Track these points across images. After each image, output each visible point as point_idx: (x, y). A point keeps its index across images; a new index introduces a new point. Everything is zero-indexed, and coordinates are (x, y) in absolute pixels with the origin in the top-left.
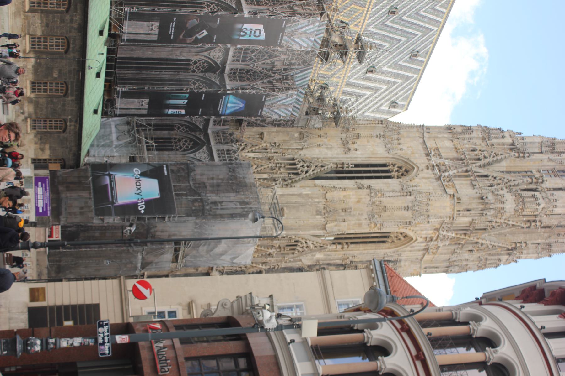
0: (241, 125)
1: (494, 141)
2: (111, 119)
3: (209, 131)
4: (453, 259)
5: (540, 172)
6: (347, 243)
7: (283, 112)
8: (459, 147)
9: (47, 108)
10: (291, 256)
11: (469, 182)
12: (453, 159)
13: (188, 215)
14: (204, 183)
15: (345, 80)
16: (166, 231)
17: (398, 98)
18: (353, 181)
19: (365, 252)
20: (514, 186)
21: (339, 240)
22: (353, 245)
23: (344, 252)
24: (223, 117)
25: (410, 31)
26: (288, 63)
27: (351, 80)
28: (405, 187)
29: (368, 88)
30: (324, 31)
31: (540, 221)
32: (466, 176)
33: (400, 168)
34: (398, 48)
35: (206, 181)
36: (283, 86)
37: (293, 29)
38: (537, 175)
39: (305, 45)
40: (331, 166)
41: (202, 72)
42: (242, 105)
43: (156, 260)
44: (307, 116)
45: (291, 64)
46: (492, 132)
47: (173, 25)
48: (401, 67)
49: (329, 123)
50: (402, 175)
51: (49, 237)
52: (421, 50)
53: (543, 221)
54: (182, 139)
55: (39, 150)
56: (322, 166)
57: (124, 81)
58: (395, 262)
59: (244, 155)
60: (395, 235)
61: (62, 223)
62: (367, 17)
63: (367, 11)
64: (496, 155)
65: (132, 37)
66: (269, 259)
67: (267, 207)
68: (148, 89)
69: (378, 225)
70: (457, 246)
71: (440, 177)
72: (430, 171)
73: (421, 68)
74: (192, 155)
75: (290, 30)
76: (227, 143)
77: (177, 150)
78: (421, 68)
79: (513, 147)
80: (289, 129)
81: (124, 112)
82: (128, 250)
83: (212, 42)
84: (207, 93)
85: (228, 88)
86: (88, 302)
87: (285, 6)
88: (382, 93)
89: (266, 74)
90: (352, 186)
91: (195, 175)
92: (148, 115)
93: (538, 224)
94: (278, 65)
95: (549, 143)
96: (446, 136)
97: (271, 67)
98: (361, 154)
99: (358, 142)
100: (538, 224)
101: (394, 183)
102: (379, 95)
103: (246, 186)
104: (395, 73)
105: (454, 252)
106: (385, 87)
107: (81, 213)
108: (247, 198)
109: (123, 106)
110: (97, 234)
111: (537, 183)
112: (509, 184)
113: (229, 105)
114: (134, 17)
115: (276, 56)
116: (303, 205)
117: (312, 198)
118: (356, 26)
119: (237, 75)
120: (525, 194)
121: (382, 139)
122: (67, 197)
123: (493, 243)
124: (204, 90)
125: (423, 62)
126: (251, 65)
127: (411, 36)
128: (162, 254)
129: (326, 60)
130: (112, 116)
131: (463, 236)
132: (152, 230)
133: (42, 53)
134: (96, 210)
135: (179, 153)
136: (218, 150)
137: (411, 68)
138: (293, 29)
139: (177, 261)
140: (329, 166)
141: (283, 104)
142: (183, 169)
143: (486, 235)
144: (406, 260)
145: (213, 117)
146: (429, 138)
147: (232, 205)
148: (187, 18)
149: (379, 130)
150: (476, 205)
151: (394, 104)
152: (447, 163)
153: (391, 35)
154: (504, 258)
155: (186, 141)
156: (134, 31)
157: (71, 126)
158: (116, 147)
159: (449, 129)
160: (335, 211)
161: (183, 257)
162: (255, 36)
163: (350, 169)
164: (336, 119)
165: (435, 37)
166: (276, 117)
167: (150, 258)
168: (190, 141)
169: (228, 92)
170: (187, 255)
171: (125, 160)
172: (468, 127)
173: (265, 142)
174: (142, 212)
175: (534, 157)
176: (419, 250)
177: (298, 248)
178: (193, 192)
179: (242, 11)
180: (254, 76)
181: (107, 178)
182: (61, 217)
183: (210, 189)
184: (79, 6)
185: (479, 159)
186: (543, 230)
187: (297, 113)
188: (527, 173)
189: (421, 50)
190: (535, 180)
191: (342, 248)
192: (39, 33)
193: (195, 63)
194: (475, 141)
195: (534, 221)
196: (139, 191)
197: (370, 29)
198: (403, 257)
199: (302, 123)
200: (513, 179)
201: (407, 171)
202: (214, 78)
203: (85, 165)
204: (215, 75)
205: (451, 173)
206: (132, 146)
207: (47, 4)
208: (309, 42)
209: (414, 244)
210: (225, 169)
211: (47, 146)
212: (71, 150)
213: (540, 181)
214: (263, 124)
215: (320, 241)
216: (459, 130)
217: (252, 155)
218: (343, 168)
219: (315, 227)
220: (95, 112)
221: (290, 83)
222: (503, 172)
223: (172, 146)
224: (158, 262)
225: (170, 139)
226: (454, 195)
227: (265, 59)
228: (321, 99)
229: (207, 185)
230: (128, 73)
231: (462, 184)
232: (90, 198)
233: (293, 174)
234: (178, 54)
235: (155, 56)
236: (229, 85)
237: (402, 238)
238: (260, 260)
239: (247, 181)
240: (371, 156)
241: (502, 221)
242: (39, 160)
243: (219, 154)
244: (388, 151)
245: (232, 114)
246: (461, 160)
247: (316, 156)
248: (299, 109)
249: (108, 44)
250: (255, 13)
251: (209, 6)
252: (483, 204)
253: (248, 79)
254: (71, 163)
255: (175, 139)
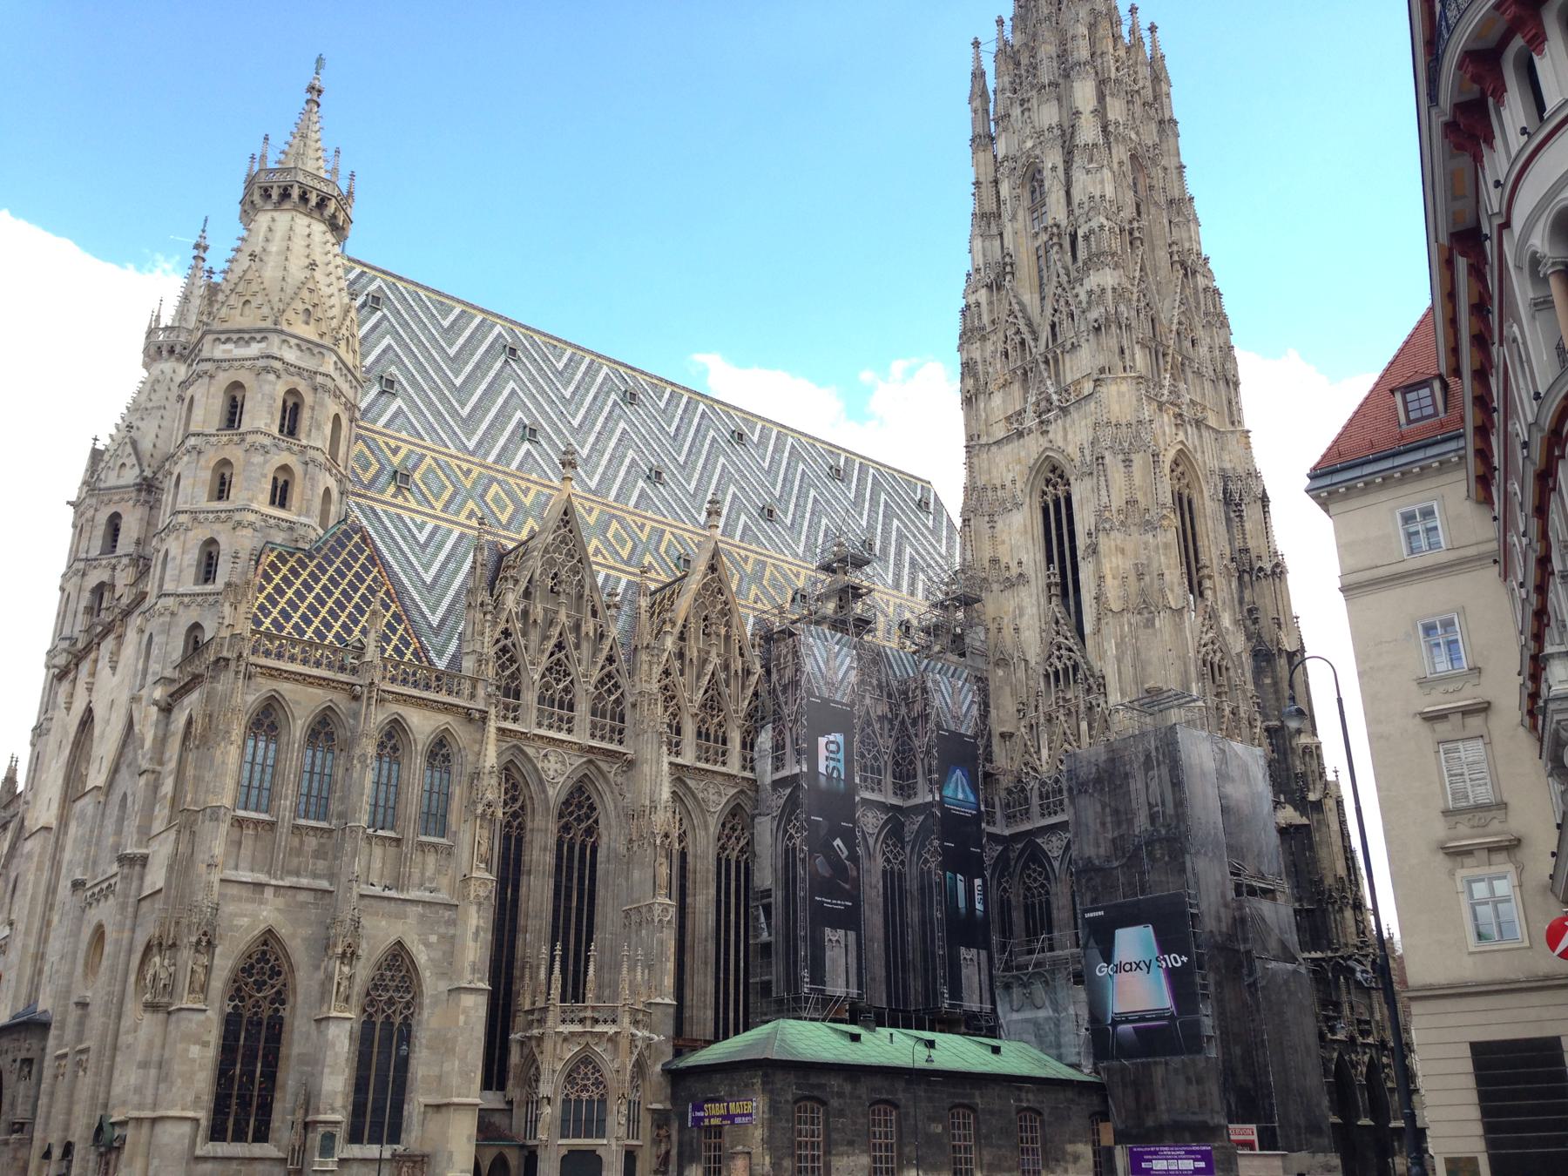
0: (992, 775)
1: (986, 319)
2: (1002, 1021)
3: (1007, 832)
4: (1212, 373)
5: (1037, 234)
6: (1198, 570)
7: (965, 698)
8: (1001, 381)
9: (999, 1147)
10: (1232, 673)
11: (1067, 356)
12: (1026, 390)
13: (1183, 870)
14: (1114, 840)
15: (890, 591)
16: (1218, 912)
17: (912, 499)
18: (1082, 565)
19: (1211, 535)
20: (1068, 276)
21: (1196, 586)
22: (1201, 557)
23: (1216, 575)
24: (983, 808)
25: (797, 483)
26: (878, 692)
27: (890, 582)
28: (1085, 469)
29: (899, 553)
30: (819, 628)
31: (1131, 222)
32: (1056, 361)
33: (1048, 482)
34: (827, 501)
35: (1110, 836)
36: (919, 698)
37: (822, 683)
38: (1045, 237)
39: (848, 659)
40: (1056, 606)
41: (903, 848)
42: (958, 772)
43: (1277, 931)
44: (968, 654)
45: (880, 686)
46: (969, 325)
47: (828, 903)
48: (860, 494)
49: (975, 615)
50: (1061, 476)
51: (1252, 1148)
52: (827, 463)
53: (1130, 217)
54: (1025, 883)
55: (1078, 1165)
56: (1057, 622)
57: (931, 994)
58: (1225, 478)
59: (1045, 767)
60: (1175, 482)
61: (1223, 1121)
62: (782, 557)
63: (771, 557)
64: (1011, 312)
65: (853, 979)
66: (1242, 715)
67: (1148, 720)
68: (943, 948)
69: (1165, 512)
70: (1187, 369)
71: (1061, 409)
72: (1051, 428)
73: (858, 460)
74: (1056, 864)
75: (824, 688)
76: (1026, 799)
77: (1047, 893)
78: (858, 460)
79: (995, 286)
80: (991, 687)
81: (986, 995)
82: (1263, 987)
83: (853, 830)
84: (942, 839)
85: (929, 798)
86: (1468, 1066)
87: (782, 699)
88: (906, 526)
89: (900, 730)
90: (1091, 566)
91: (1098, 857)
92: (987, 946)
93: (1135, 225)
94: (882, 709)
95: (983, 223)
96: (982, 405)
97: (886, 723)
98: (1027, 553)
99: (1004, 560)
100: (1135, 225)
101: (1080, 491)
102: (910, 531)
103: (1112, 760)
104: (871, 505)
105: (1198, 374)
106: (896, 522)
107: (1199, 1081)
108: (1137, 756)
109: (976, 997)
110: (1237, 1051)
111: (1059, 235)
112: (1065, 285)
113: (960, 796)
114: (818, 976)
115: (868, 713)
116: (1137, 654)
117: (1123, 637)
118: (797, 575)
119: (904, 781)
120: (1082, 254)
121: (996, 518)
122: (1169, 1111)
123: (1177, 303)
124: (936, 843)
125: (847, 458)
126: (886, 757)
127: (806, 480)
128: (1263, 920)
129: (868, 623)
130: (997, 1017)
131: (1169, 359)
132: (1219, 938)
133: (900, 1155)
134: (1190, 1052)
135: (1054, 888)
136: (1043, 815)
137: (858, 480)
138: (822, 683)
139: (1272, 891)
140: (1056, 609)
141: (951, 697)
142: (1089, 880)
143: (1162, 316)
144: (1220, 459)
145: (983, 825)
146: (988, 434)
147: (1154, 785)
148: (814, 876)
149: (981, 523)
150: (1111, 340)
151: (923, 505)
152: (1034, 399)
153: (808, 515)
154: (1201, 281)
155: (1029, 876)
156: (843, 976)
157: (1030, 1099)
158: (1056, 1010)
159: (969, 401)
160: (1143, 592)
161: (1263, 877)
162: (838, 751)
163: (1057, 571)
164: (967, 602)
165: (803, 439)
166: (975, 707)
167: (1273, 944)
168: (1029, 868)
169: (937, 798)
170: (1260, 871)
171: (1081, 993)
172: (963, 368)
173: (1018, 729)
174: (1185, 959)
175: (1011, 250)
176: (1201, 436)
177: (1216, 659)
178: (1133, 859)
179: (797, 775)
180: (904, 753)
181: (1121, 1028)
182: (1211, 1123)
183: (1124, 826)
184: (813, 1080)
185: (1023, 342)
186: (1144, 216)
187: (962, 672)
188: (1042, 255)
189: (827, 463)
190: (1055, 240)
191: (1210, 577)
192: (865, 1160)
193: (888, 860)
194: (988, 354)
195: (1131, 234)
196: (1142, 965)
197: (800, 551)
198: (1213, 464)
199: (980, 663)
200: (1055, 279)
201: (1054, 470)
202: (913, 825)
203: (1098, 1073)
204: (907, 823)
205: (1051, 390)
206: (1054, 980)
207: (813, 1143)
208: (843, 653)
209: (1191, 447)
210: (1083, 801)
211: (1070, 1148)
212: (1073, 1100)
213: (1055, 230)
214: (986, 733)
215: (1201, 619)
216: (970, 382)
217: (1045, 753)
218: (1056, 584)
219: (1179, 628)
220: (996, 1050)
221: (913, 686)
222: (1043, 299)
223: (1041, 903)
224: (1280, 929)
225: (1026, 906)
226: (1096, 381)
227: (874, 732)
228: (932, 631)
229: (1116, 834)
230: (915, 985)
231: (1071, 368)
232: (1166, 1064)
233: (1075, 675)
234: (874, 893)
235: (880, 934)
236: (924, 796)
237: (1180, 469)
238: (1246, 731)
239: (1103, 757)
240: (1030, 536)
241: (1135, 290)
242: (1096, 1166)
243: (1050, 814)
244: (1018, 506)
245: (975, 790)
246: (1025, 374)
247: (1038, 636)
248: (956, 669)
249: (872, 1025)
250: (799, 752)
251: (791, 837)
252: (1108, 327)
253: (911, 763)
254: (1096, 1099)
255: (1026, 897)
